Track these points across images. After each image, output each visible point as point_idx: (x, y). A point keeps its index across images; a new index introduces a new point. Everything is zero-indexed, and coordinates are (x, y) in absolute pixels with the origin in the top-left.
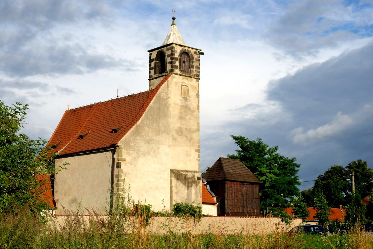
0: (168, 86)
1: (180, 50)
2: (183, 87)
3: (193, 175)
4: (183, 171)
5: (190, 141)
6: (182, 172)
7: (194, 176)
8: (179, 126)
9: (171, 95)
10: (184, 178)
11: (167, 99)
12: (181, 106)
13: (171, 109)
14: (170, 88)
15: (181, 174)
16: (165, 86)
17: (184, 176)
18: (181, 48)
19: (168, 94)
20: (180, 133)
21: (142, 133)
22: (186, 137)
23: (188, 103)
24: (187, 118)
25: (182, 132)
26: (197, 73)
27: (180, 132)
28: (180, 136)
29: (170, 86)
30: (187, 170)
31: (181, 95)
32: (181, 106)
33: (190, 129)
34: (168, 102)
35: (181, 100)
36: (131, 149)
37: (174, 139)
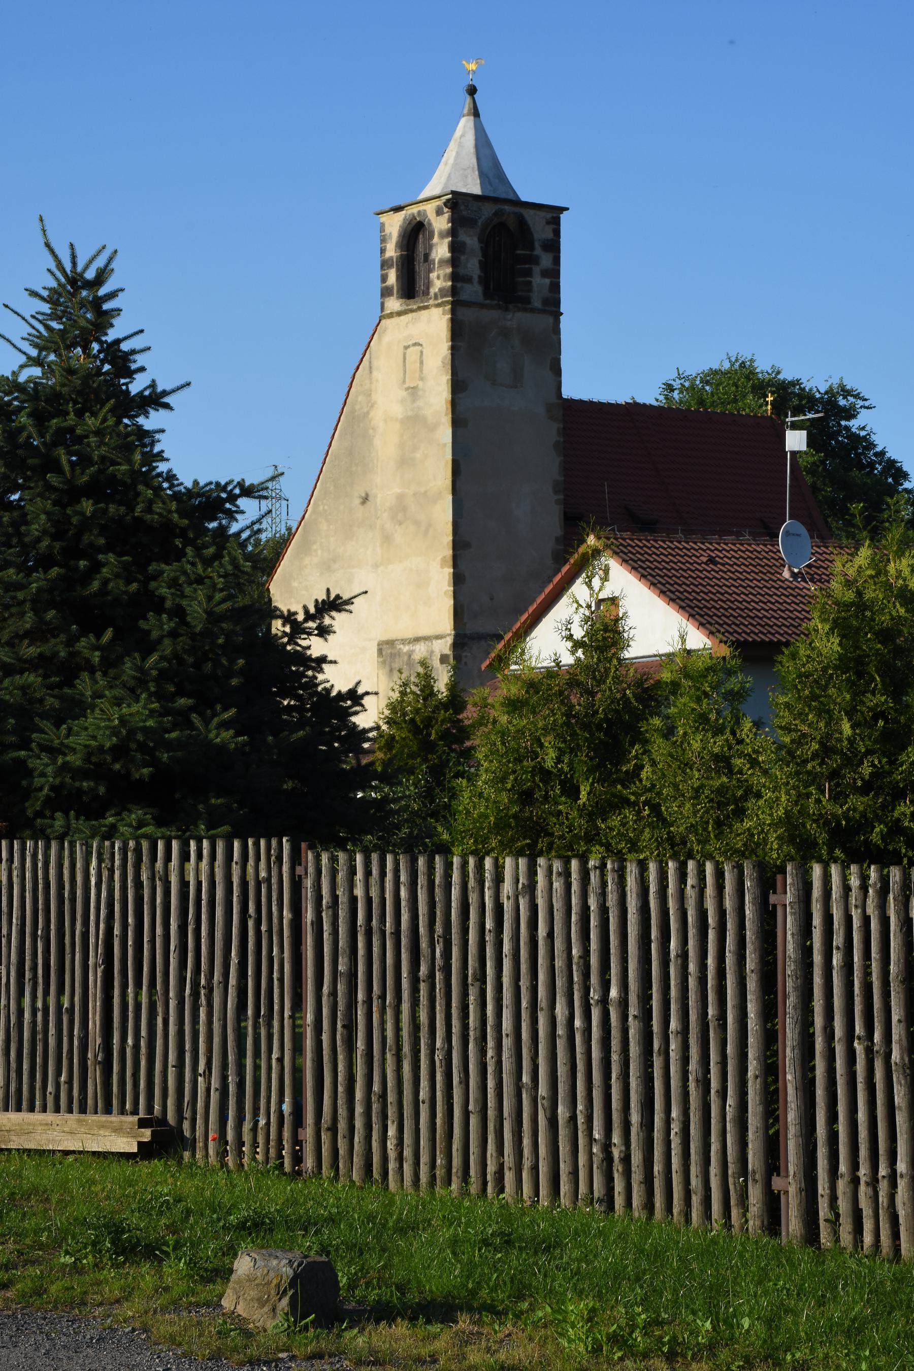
0: (370, 368)
1: (400, 223)
2: (409, 351)
3: (428, 651)
4: (404, 641)
5: (426, 532)
6: (402, 646)
7: (432, 652)
8: (399, 491)
9: (378, 397)
10: (407, 664)
11: (368, 413)
12: (402, 422)
13: (377, 442)
14: (375, 373)
15: (399, 654)
16: (364, 368)
17: (406, 658)
18: (401, 215)
19: (370, 395)
20: (400, 516)
21: (315, 543)
22: (417, 523)
23: (420, 403)
24: (418, 455)
25: (404, 509)
26: (444, 284)
27: (400, 511)
28: (400, 524)
29: (375, 363)
30: (420, 634)
31: (404, 382)
32: (402, 422)
33: (426, 492)
34: (370, 422)
35: (403, 401)
36: (293, 600)
37: (387, 539)
